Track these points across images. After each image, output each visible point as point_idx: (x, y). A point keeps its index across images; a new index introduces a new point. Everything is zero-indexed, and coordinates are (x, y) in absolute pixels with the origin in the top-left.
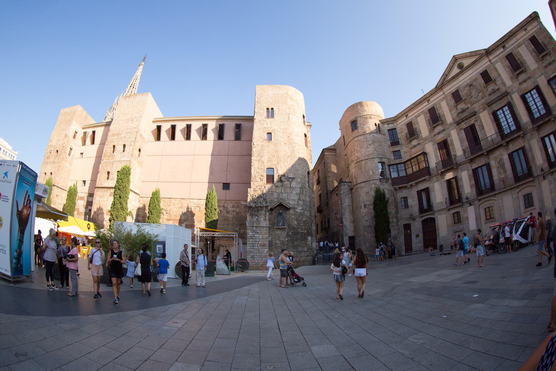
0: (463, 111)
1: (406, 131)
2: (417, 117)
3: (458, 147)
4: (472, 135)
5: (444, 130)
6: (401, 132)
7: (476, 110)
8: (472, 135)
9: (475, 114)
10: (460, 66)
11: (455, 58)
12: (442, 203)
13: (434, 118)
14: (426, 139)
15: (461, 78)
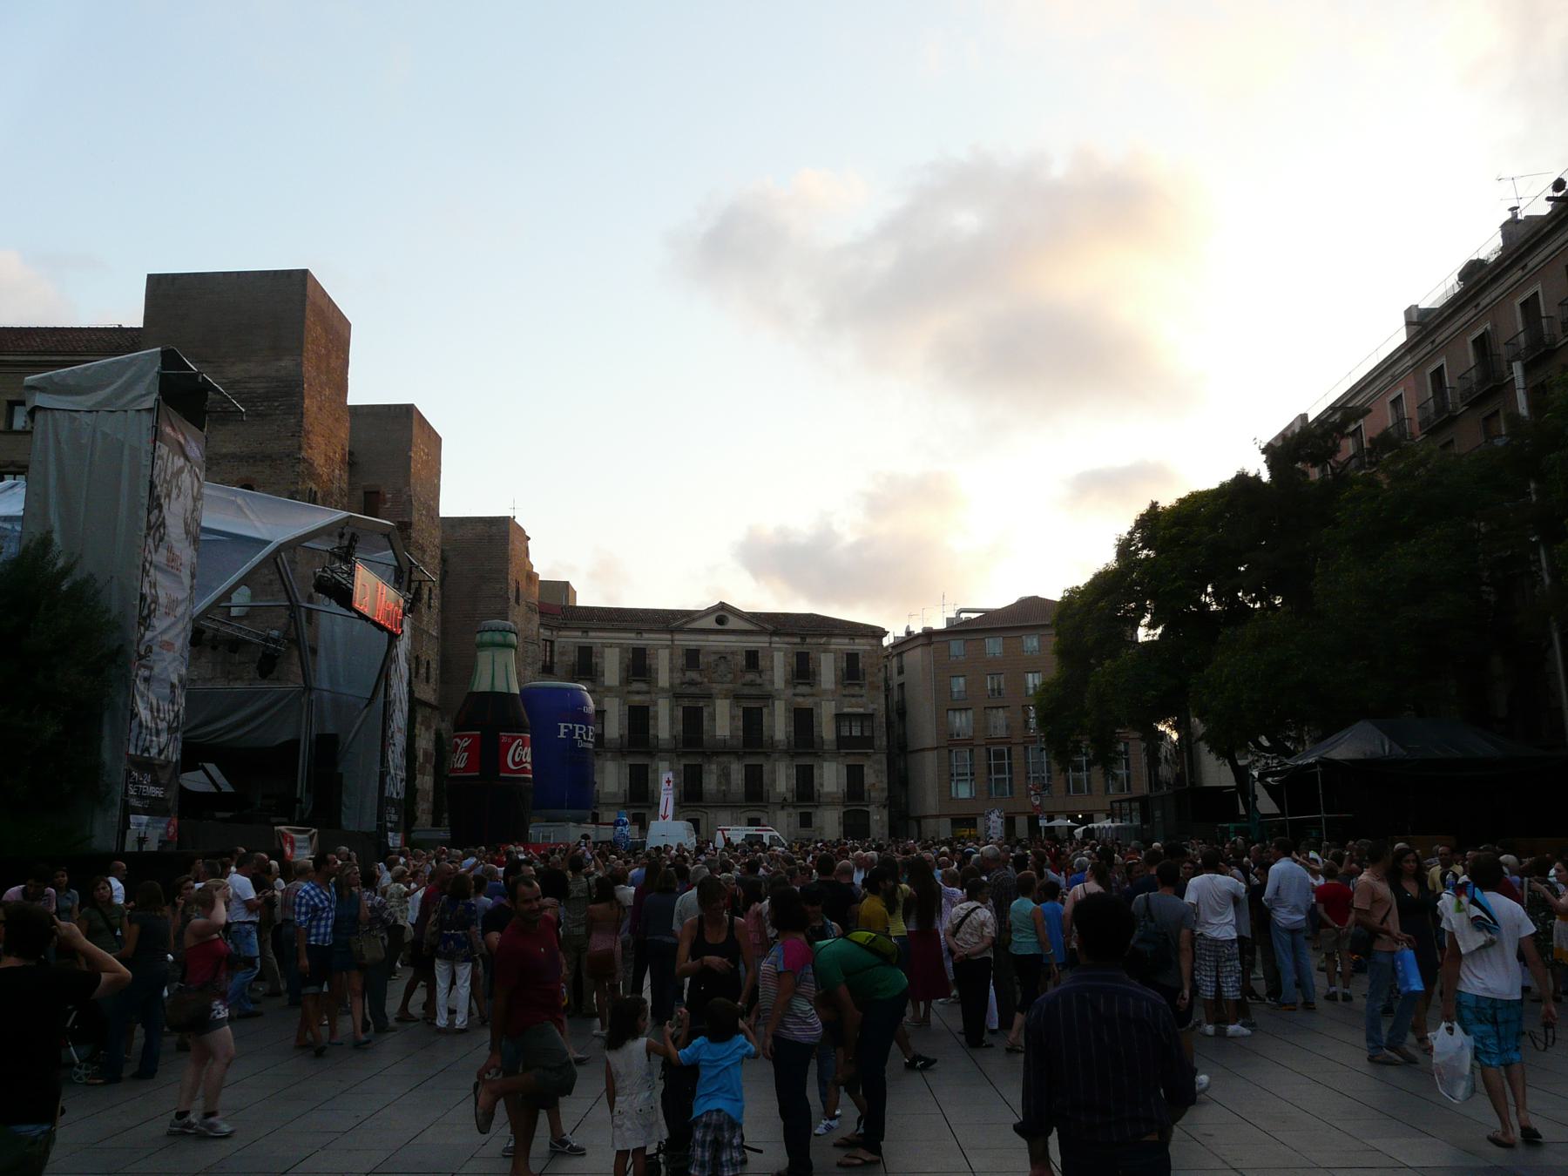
0: (692, 683)
1: (572, 657)
2: (604, 646)
3: (664, 725)
4: (693, 720)
5: (648, 693)
6: (562, 654)
7: (714, 691)
8: (693, 720)
9: (709, 696)
10: (720, 621)
11: (722, 606)
12: (615, 795)
13: (638, 666)
14: (609, 689)
15: (712, 637)
